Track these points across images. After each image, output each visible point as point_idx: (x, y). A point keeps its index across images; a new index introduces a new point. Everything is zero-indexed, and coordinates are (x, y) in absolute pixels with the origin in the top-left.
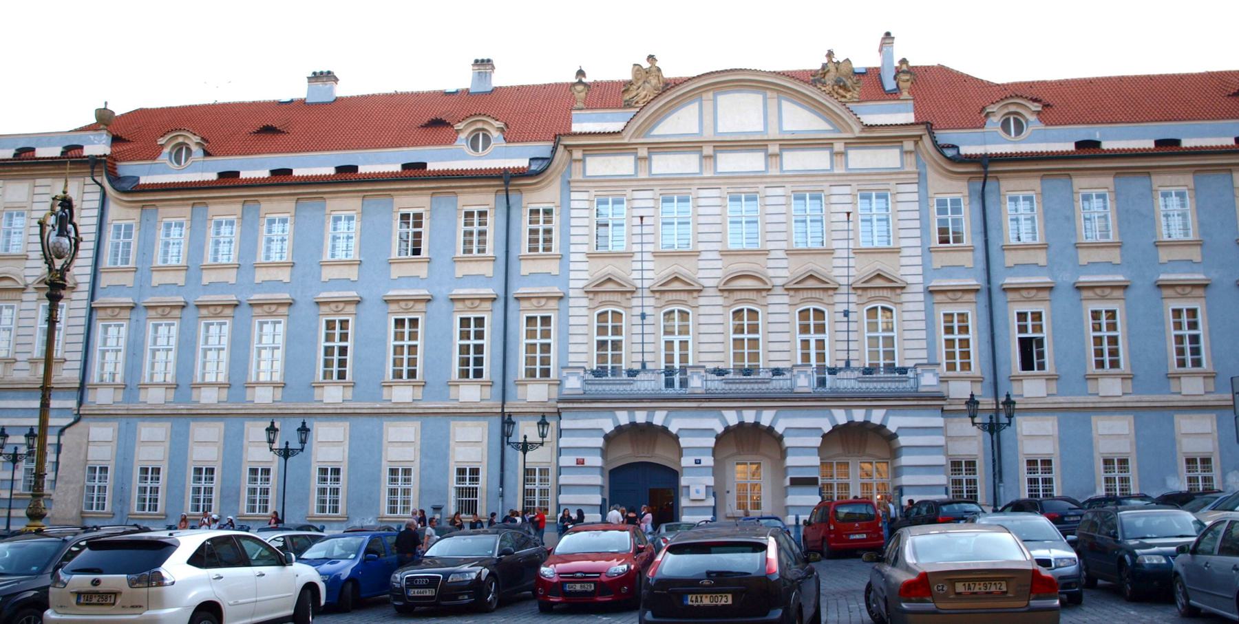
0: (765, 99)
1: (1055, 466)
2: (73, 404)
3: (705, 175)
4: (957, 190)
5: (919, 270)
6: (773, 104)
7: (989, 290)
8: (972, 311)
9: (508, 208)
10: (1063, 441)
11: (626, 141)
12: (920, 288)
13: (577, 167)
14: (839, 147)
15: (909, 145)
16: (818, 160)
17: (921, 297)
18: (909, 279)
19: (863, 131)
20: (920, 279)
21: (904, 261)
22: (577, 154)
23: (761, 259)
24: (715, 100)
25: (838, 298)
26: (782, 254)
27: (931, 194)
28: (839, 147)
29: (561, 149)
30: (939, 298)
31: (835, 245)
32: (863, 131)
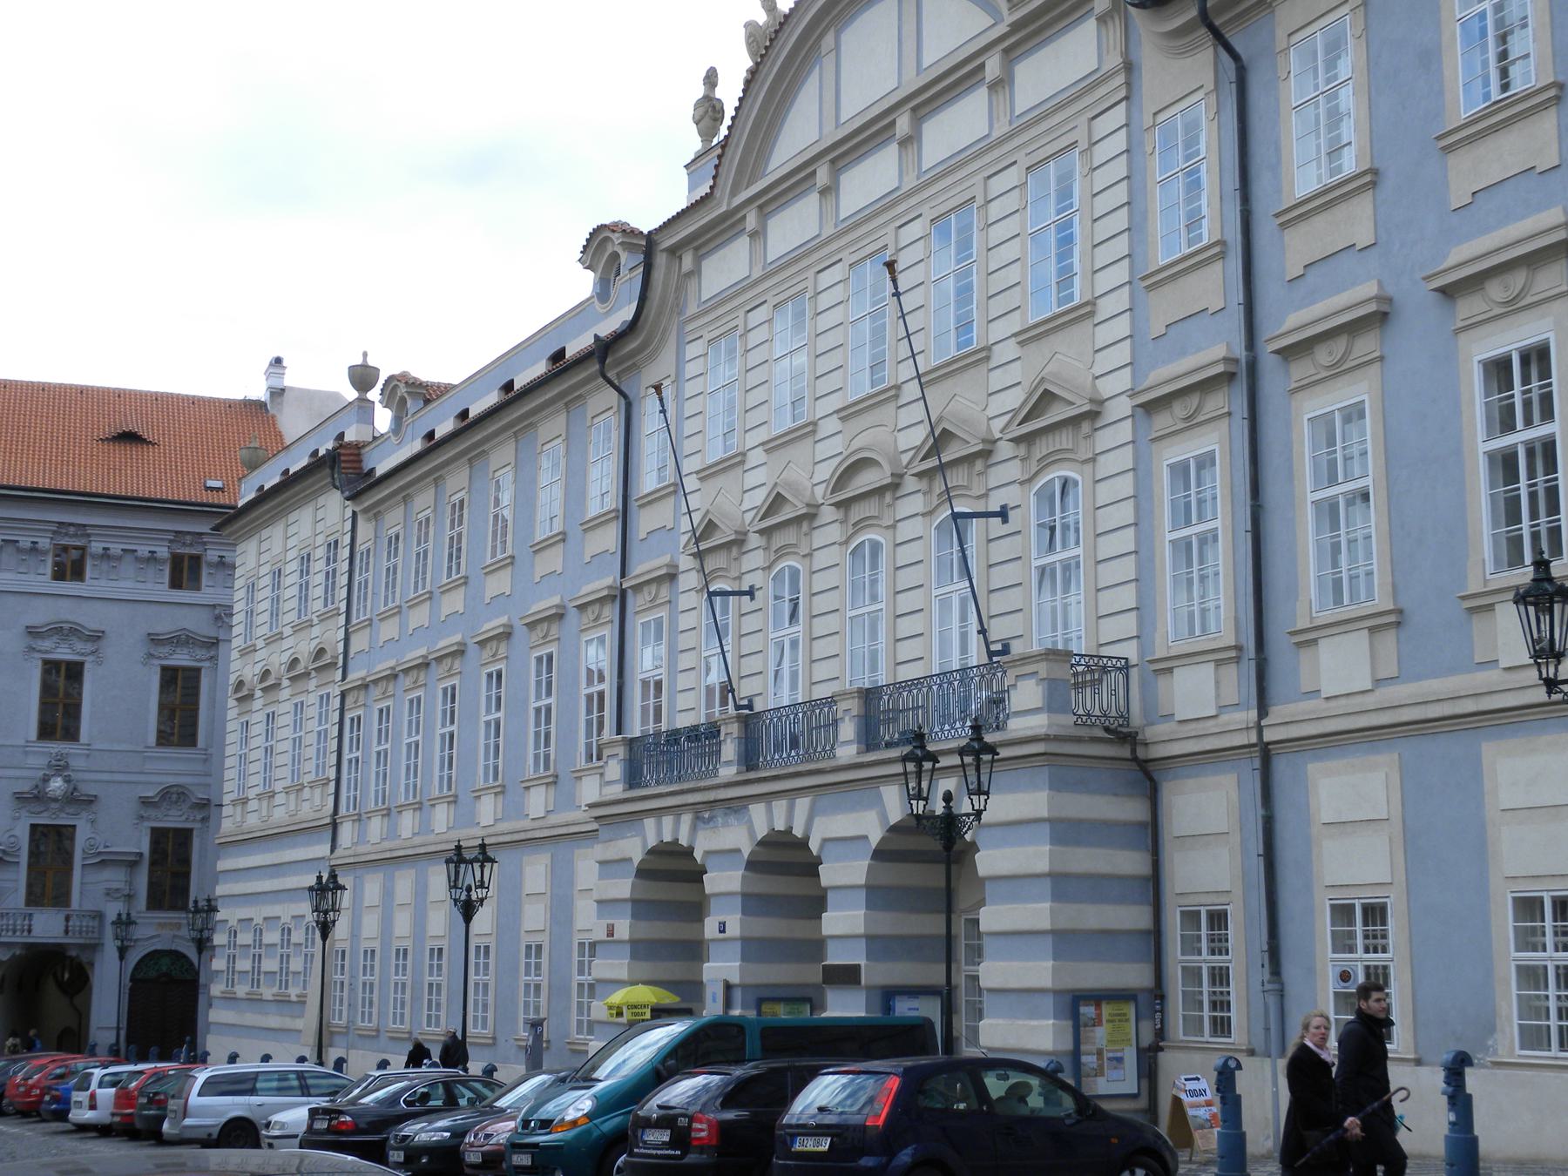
1: (1394, 925)
2: (323, 850)
8: (1215, 441)
9: (629, 406)
10: (1415, 843)
11: (724, 208)
12: (1123, 407)
13: (692, 284)
17: (1125, 432)
18: (1107, 387)
22: (688, 261)
24: (837, 47)
29: (661, 260)
30: (1163, 422)
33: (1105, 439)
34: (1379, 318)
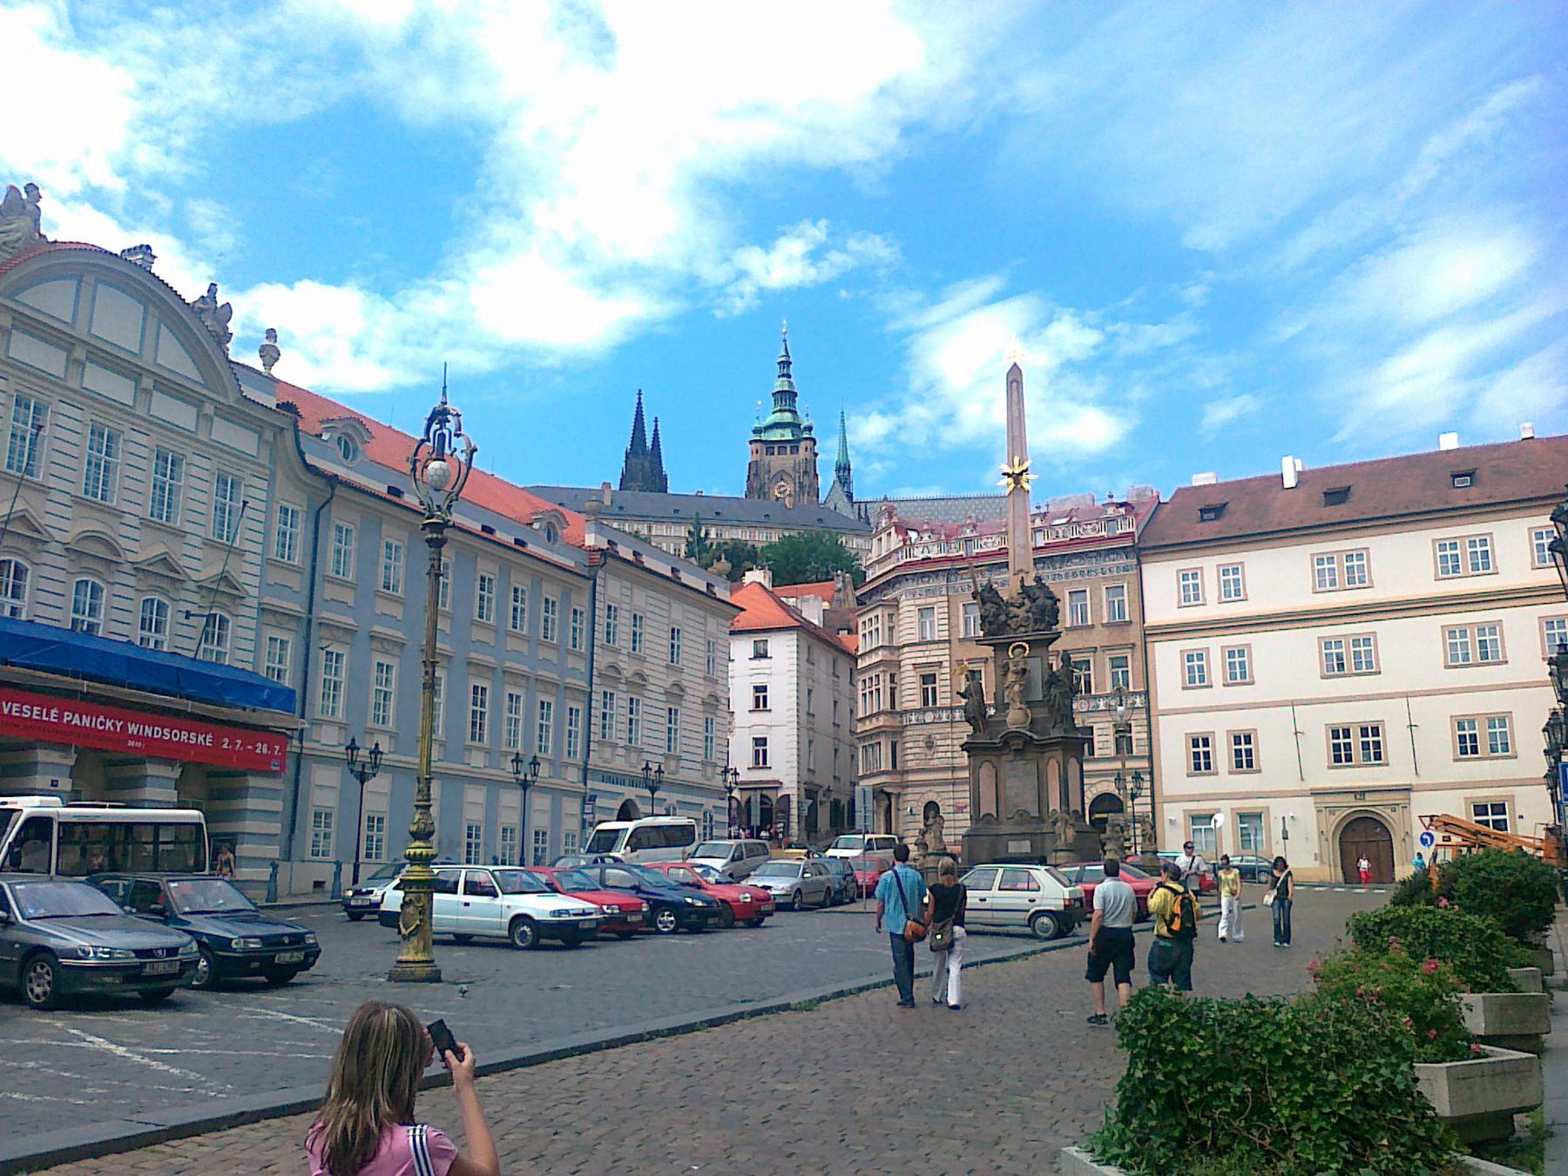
0: (146, 311)
3: (70, 384)
4: (298, 503)
5: (256, 582)
6: (152, 322)
7: (310, 621)
14: (209, 409)
15: (268, 435)
16: (183, 416)
17: (254, 613)
19: (237, 402)
20: (254, 592)
21: (247, 568)
23: (114, 521)
25: (183, 595)
26: (135, 522)
27: (278, 496)
28: (209, 409)
30: (269, 618)
31: (189, 527)
32: (237, 402)
33: (242, 611)
34: (351, 632)
